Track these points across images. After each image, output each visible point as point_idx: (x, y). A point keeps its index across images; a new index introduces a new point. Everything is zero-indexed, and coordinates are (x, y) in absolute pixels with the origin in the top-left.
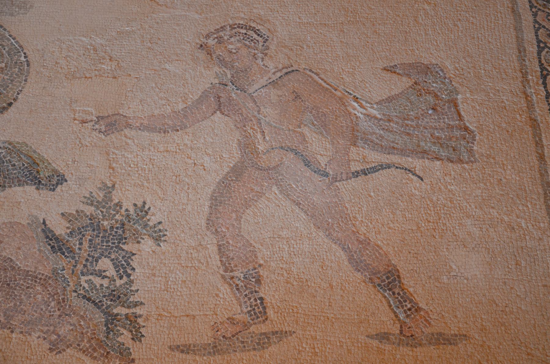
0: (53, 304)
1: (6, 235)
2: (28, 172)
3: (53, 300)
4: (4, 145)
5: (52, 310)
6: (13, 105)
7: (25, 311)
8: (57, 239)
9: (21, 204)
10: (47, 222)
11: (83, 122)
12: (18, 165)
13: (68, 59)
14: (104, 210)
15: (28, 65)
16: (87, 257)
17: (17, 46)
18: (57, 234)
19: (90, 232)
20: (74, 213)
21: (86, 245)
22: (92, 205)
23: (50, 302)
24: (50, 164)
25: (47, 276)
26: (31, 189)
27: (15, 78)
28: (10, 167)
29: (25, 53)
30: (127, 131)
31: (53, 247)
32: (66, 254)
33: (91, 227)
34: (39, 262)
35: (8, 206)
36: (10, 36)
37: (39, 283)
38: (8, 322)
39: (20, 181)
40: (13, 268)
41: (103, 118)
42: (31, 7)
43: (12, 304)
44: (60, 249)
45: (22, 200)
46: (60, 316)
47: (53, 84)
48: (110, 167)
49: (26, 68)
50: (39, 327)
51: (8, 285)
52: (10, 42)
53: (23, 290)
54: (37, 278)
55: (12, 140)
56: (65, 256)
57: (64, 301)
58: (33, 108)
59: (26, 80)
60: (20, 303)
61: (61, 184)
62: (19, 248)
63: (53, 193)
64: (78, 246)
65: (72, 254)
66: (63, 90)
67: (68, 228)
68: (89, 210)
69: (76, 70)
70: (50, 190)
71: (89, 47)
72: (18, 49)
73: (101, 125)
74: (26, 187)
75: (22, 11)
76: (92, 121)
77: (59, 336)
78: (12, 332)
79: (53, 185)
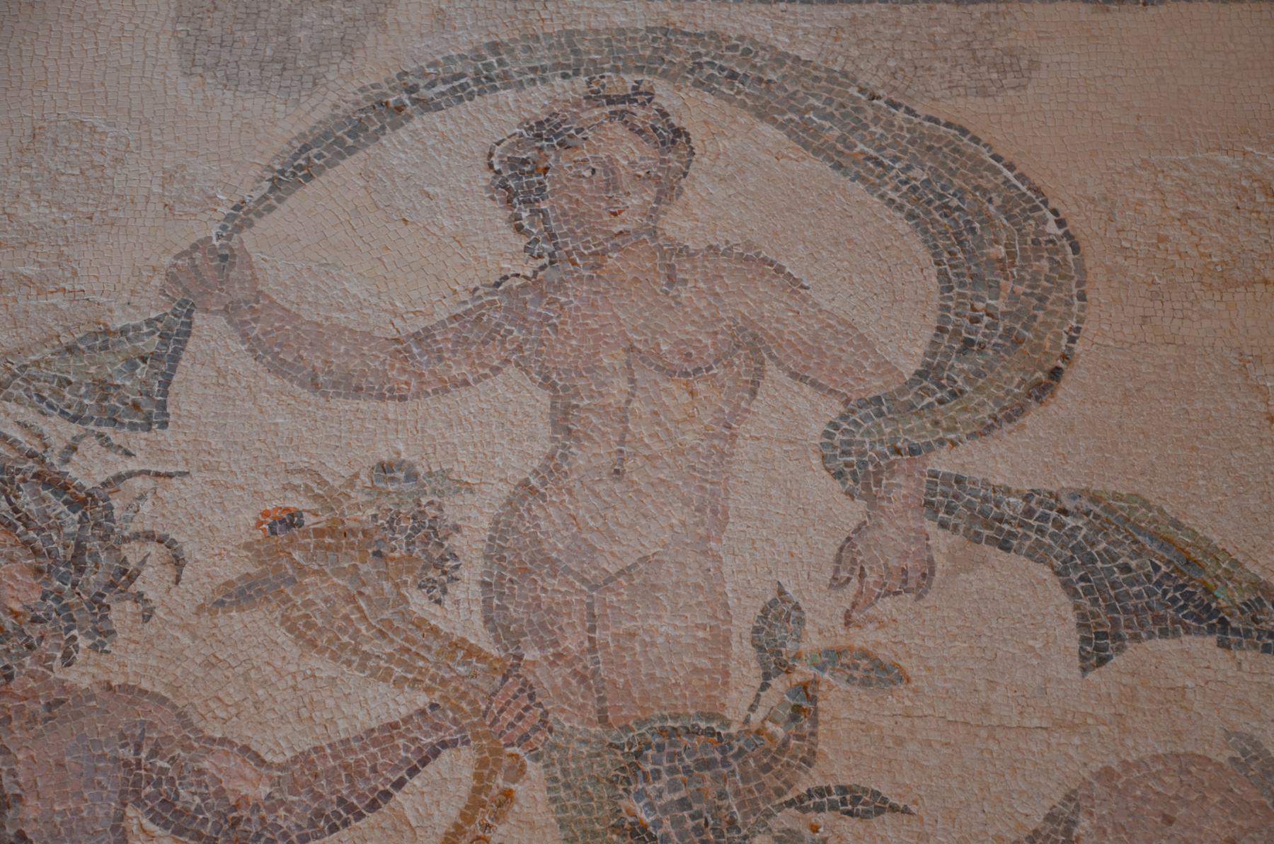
1: (1177, 797)
2: (1176, 589)
4: (1077, 502)
6: (1067, 377)
9: (1190, 695)
12: (1140, 567)
13: (1192, 223)
15: (1076, 249)
17: (1024, 189)
24: (1235, 563)
26: (1203, 645)
27: (1049, 290)
28: (1118, 575)
29: (1055, 212)
35: (1150, 701)
36: (998, 158)
39: (1163, 619)
42: (1034, 65)
45: (1189, 683)
47: (1168, 305)
49: (1070, 257)
52: (1000, 180)
55: (1097, 486)
58: (1129, 385)
59: (1082, 297)
66: (1206, 323)
69: (1227, 258)
71: (1244, 183)
72: (1030, 200)
74: (1186, 638)
75: (1010, 80)
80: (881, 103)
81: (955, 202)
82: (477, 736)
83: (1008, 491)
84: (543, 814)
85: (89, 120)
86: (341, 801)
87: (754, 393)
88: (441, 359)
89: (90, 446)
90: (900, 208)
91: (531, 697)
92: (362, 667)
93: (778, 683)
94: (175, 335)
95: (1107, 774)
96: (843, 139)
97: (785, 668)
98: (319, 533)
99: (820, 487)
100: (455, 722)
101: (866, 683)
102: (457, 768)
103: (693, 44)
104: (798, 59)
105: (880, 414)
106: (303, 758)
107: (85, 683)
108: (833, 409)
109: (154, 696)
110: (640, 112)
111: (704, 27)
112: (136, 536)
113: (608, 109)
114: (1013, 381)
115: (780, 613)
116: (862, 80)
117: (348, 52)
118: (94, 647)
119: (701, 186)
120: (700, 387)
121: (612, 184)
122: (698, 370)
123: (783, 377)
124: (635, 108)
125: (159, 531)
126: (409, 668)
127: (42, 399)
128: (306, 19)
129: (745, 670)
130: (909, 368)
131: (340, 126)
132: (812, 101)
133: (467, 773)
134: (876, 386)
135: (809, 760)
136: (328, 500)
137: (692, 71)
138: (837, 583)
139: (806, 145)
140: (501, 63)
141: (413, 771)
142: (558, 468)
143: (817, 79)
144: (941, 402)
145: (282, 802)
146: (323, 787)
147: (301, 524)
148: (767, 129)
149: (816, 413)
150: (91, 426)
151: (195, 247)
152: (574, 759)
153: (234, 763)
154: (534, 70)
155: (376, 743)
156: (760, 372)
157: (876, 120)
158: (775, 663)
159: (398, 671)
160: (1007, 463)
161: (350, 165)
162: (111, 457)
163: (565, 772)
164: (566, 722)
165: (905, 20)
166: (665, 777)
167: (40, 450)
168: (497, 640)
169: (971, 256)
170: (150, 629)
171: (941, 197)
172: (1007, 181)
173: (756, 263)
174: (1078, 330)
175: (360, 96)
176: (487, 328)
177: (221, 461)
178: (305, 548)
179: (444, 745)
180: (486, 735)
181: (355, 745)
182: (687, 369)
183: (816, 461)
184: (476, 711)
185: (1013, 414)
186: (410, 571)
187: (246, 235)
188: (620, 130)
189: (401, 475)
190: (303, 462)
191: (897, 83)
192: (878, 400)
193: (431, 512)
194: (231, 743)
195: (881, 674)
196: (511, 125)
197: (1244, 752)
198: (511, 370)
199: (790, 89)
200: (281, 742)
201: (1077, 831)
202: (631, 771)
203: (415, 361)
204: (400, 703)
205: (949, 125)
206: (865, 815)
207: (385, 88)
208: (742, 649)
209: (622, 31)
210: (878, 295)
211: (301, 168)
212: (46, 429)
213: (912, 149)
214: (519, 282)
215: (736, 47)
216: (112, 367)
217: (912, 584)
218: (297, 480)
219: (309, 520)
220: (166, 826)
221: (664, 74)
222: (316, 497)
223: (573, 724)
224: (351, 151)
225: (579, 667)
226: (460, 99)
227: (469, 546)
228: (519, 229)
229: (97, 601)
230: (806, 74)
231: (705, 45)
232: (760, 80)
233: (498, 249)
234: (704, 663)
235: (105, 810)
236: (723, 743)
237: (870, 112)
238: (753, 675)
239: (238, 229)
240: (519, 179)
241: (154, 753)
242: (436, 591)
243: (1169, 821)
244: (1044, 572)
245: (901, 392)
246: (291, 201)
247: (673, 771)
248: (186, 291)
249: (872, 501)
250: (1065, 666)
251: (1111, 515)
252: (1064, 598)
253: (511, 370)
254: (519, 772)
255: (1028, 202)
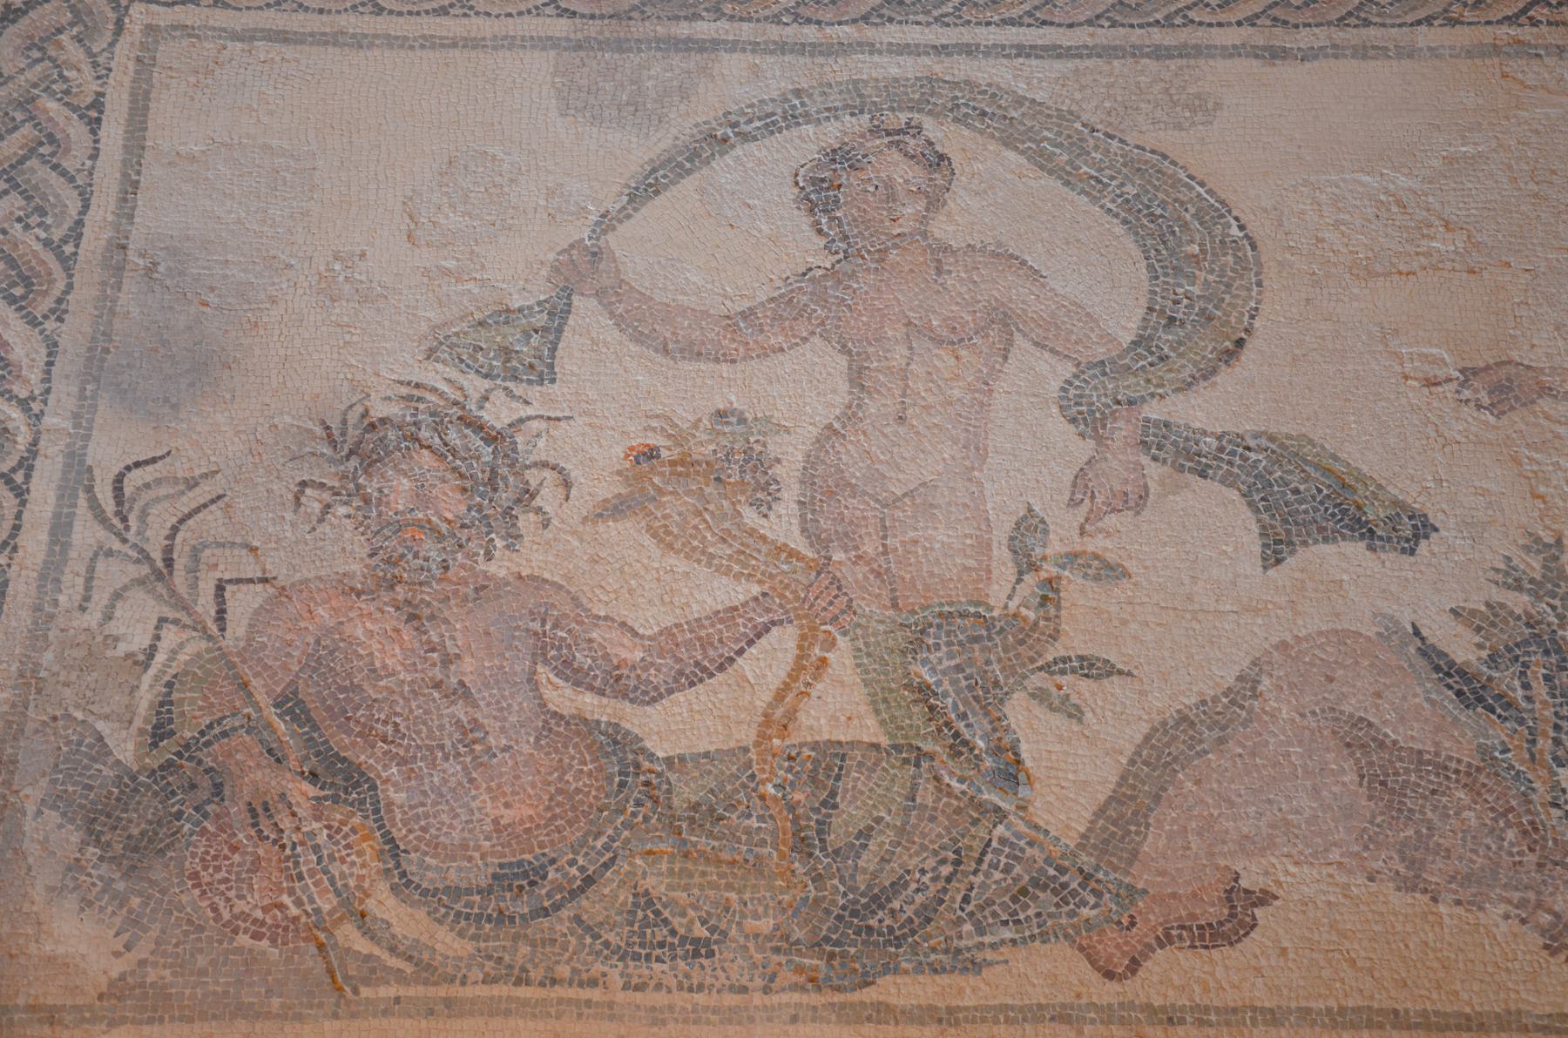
0: (1511, 835)
1: (1336, 662)
2: (1335, 506)
3: (1509, 825)
4: (1258, 441)
5: (1515, 850)
6: (1248, 345)
7: (1448, 850)
8: (1462, 673)
9: (1346, 586)
10: (1425, 632)
11: (1431, 383)
12: (1307, 490)
13: (1343, 228)
14: (1557, 602)
15: (1254, 247)
16: (1554, 719)
17: (1212, 201)
18: (1458, 661)
19: (1539, 656)
20: (1483, 608)
21: (1540, 690)
22: (1519, 588)
23: (1502, 830)
24: (1380, 487)
25: (1469, 765)
26: (1355, 549)
27: (1234, 279)
28: (1290, 497)
29: (1237, 219)
30: (1545, 404)
31: (1459, 693)
32: (1499, 711)
33: (1539, 645)
34: (1438, 729)
35: (1316, 591)
37: (1457, 781)
38: (1418, 877)
39: (1325, 529)
40: (1382, 745)
41: (1475, 372)
42: (1218, 106)
43: (1410, 832)
44: (1480, 699)
45: (1345, 577)
46: (1540, 866)
47: (1325, 291)
48: (1536, 496)
49: (1250, 253)
50: (1498, 891)
51: (1383, 783)
52: (1194, 195)
53: (1424, 797)
54: (1446, 768)
55: (1273, 430)
56: (1499, 716)
57: (1536, 830)
58: (1297, 352)
59: (1259, 284)
60: (1429, 829)
61: (1427, 537)
62: (1378, 695)
63: (1412, 559)
64: (1520, 692)
65: (1513, 712)
66: (1355, 304)
67: (1480, 646)
68: (1519, 602)
69: (1370, 254)
70: (1403, 551)
71: (1382, 197)
72: (1217, 210)
73: (1476, 391)
74: (1342, 544)
75: (1199, 117)
76: (1448, 380)
77: (1557, 915)
78: (1435, 900)
79: (1408, 541)
80: (1100, 135)
81: (1159, 211)
82: (798, 617)
83: (1205, 433)
84: (850, 675)
85: (490, 150)
86: (697, 664)
87: (1005, 358)
88: (762, 331)
89: (498, 397)
90: (1117, 216)
91: (839, 588)
92: (709, 565)
93: (1029, 578)
94: (559, 312)
95: (1283, 646)
96: (1070, 162)
97: (1034, 567)
98: (673, 463)
99: (1059, 429)
100: (781, 606)
101: (1097, 578)
102: (784, 640)
103: (952, 89)
104: (1034, 101)
105: (1104, 374)
106: (667, 632)
107: (502, 573)
108: (1067, 370)
109: (554, 584)
110: (912, 142)
111: (960, 76)
112: (535, 464)
113: (886, 140)
114: (1208, 348)
115: (1029, 525)
116: (1084, 117)
117: (685, 96)
118: (507, 547)
119: (960, 198)
120: (963, 353)
121: (891, 197)
122: (962, 340)
123: (1028, 345)
124: (907, 138)
125: (552, 461)
126: (745, 566)
127: (462, 361)
128: (652, 72)
129: (1004, 567)
130: (1127, 338)
131: (681, 153)
132: (1046, 133)
133: (791, 645)
134: (1100, 352)
135: (1055, 636)
136: (678, 439)
137: (951, 110)
138: (1073, 503)
139: (1042, 167)
140: (803, 104)
141: (751, 643)
142: (855, 415)
143: (1049, 116)
144: (1151, 365)
145: (652, 664)
146: (683, 653)
147: (658, 457)
148: (1011, 155)
149: (1054, 373)
150: (499, 382)
151: (572, 246)
152: (873, 634)
153: (615, 634)
154: (828, 109)
155: (721, 621)
156: (1010, 342)
157: (1096, 148)
158: (1026, 564)
159: (736, 568)
160: (1203, 411)
161: (689, 183)
162: (514, 405)
163: (866, 644)
164: (866, 606)
165: (1117, 72)
166: (944, 649)
167: (461, 399)
168: (812, 545)
169: (1172, 253)
170: (548, 534)
171: (1148, 207)
172: (1199, 195)
173: (1005, 258)
174: (1256, 309)
175: (695, 131)
176: (795, 309)
177: (595, 409)
178: (662, 474)
179: (773, 623)
180: (806, 616)
181: (706, 623)
182: (953, 339)
183: (1055, 410)
184: (797, 598)
185: (1209, 373)
186: (743, 492)
187: (610, 237)
188: (896, 156)
189: (734, 420)
190: (659, 410)
191: (1112, 120)
192: (1103, 362)
193: (758, 448)
194: (613, 620)
195: (1109, 571)
196: (812, 152)
197: (1387, 629)
198: (816, 340)
199: (1029, 124)
200: (651, 620)
201: (1260, 688)
202: (917, 644)
203: (742, 333)
204: (741, 592)
205: (1153, 152)
206: (1098, 677)
207: (714, 124)
208: (1001, 553)
209: (896, 80)
210: (1101, 283)
211: (650, 185)
212: (466, 384)
213: (1124, 170)
214: (821, 272)
215: (985, 92)
216: (513, 337)
217: (1131, 504)
218: (654, 423)
219: (664, 454)
220: (567, 680)
221: (930, 113)
222: (670, 436)
223: (872, 608)
224: (689, 172)
225: (875, 566)
226: (772, 133)
227: (788, 473)
228: (820, 232)
229: (508, 512)
230: (1041, 112)
231: (961, 90)
232: (1005, 117)
233: (803, 247)
234: (971, 563)
235: (521, 667)
236: (988, 624)
237: (1091, 142)
238: (1010, 572)
239: (604, 232)
240: (819, 193)
241: (555, 626)
242: (764, 508)
243: (1331, 680)
244: (1234, 495)
245: (1120, 357)
246: (643, 211)
247: (949, 644)
248: (567, 280)
249: (1099, 440)
250: (1250, 565)
251: (1284, 451)
252: (1249, 514)
253: (816, 340)
254: (831, 644)
255: (1216, 212)
